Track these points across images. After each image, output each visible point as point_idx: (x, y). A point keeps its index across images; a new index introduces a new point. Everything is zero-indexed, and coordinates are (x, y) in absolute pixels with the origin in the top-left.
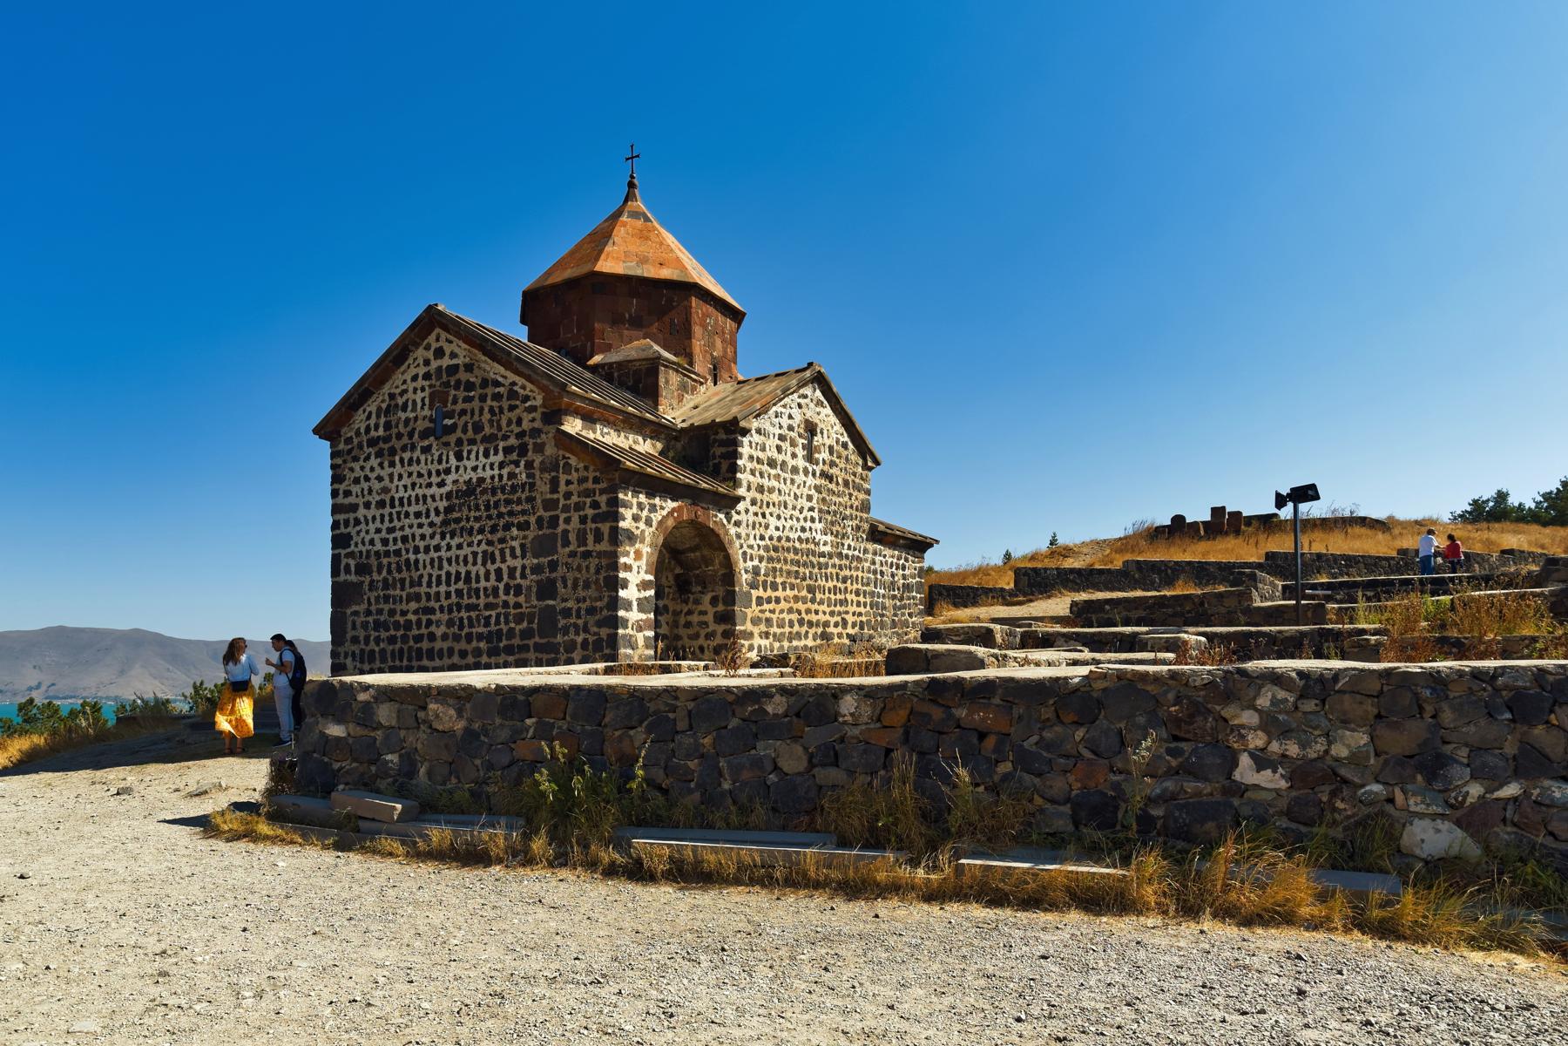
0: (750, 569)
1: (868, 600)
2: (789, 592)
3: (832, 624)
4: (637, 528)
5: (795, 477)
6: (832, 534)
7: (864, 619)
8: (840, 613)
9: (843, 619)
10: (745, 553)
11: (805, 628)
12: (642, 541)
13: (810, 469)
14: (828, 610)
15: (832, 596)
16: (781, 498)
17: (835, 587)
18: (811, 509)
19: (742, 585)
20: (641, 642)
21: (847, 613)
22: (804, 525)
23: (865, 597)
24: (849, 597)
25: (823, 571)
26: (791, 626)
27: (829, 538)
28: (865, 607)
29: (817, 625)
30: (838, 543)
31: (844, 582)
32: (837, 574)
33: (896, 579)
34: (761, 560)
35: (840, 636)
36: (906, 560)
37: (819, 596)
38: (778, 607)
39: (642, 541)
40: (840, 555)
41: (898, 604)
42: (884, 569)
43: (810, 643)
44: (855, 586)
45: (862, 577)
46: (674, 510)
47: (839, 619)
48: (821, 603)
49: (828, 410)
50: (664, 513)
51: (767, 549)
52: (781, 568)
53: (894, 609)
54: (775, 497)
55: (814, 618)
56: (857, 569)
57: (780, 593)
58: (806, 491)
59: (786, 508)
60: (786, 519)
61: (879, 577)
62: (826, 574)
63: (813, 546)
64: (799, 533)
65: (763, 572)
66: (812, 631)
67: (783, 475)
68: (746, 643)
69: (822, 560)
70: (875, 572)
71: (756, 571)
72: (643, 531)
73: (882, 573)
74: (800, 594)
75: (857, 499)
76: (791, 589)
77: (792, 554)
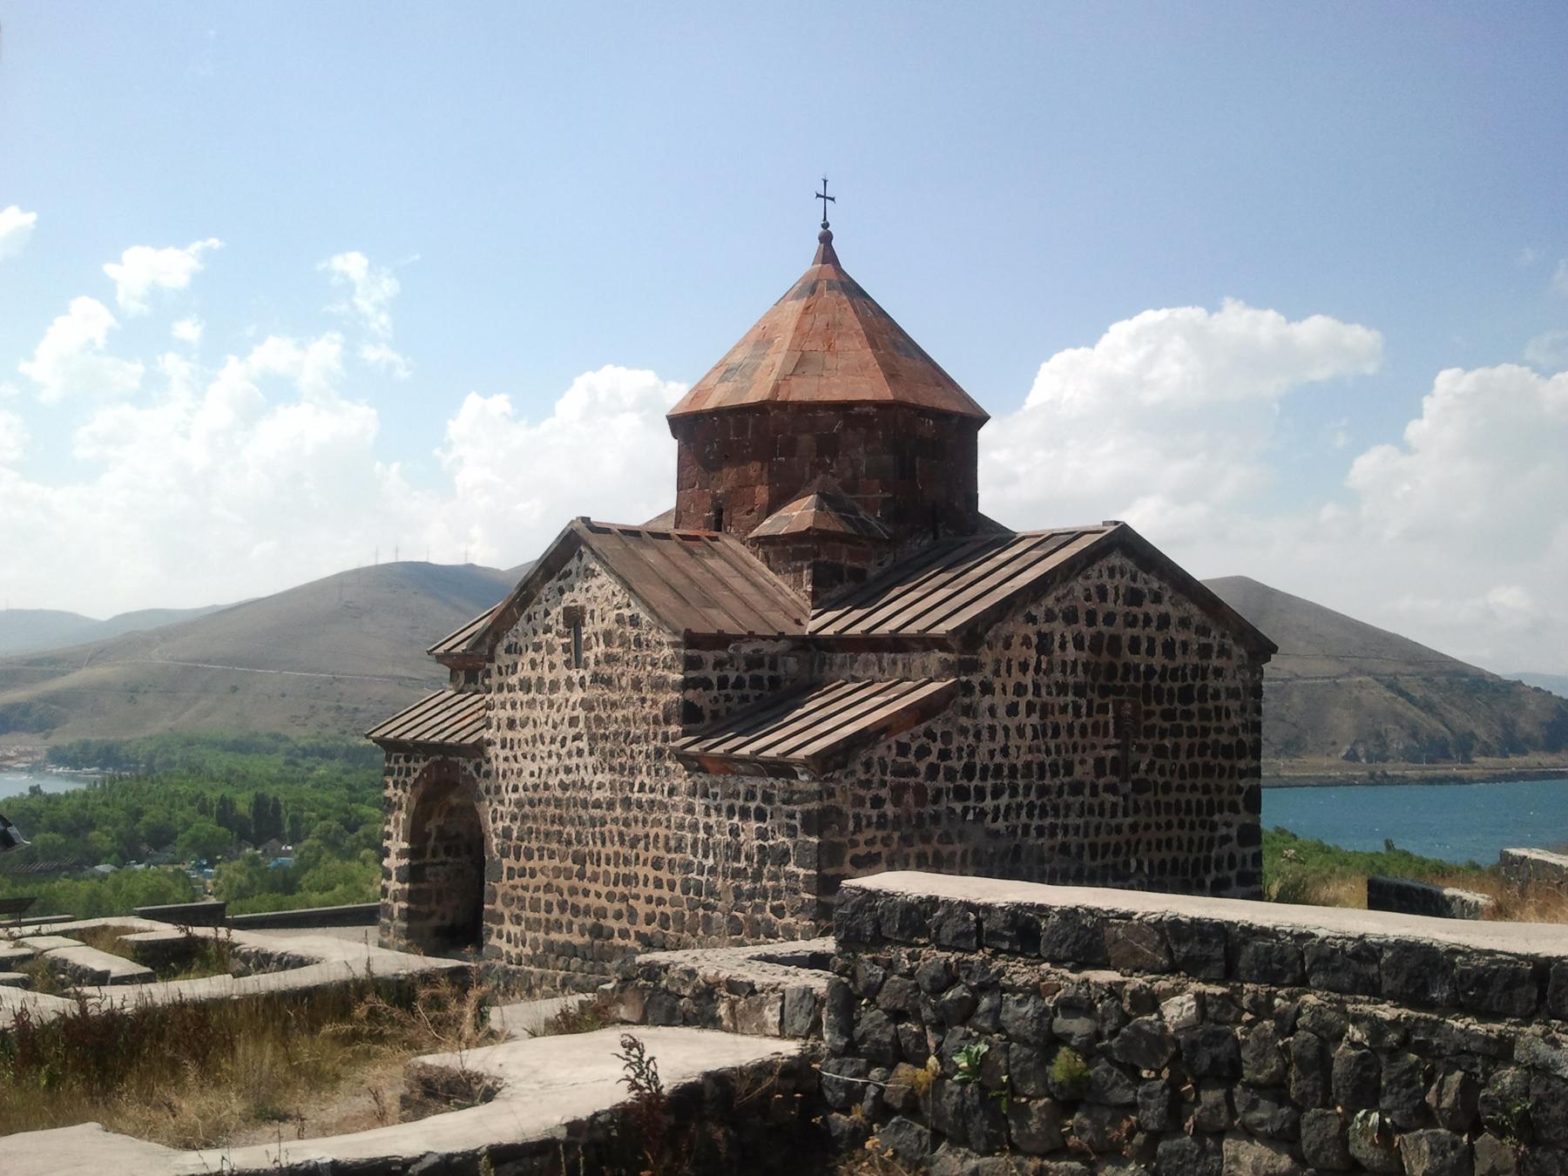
0: (500, 831)
1: (678, 877)
2: (546, 861)
3: (610, 914)
4: (396, 795)
5: (554, 697)
6: (612, 769)
7: (668, 910)
8: (624, 898)
9: (630, 908)
10: (495, 811)
11: (568, 915)
12: (400, 808)
13: (576, 679)
14: (604, 890)
15: (612, 869)
16: (539, 730)
17: (617, 854)
18: (576, 738)
19: (491, 852)
20: (396, 914)
21: (637, 897)
22: (567, 762)
23: (671, 870)
24: (642, 871)
25: (597, 829)
26: (549, 910)
27: (605, 777)
28: (672, 889)
29: (587, 912)
30: (621, 784)
31: (634, 843)
32: (621, 834)
33: (742, 837)
34: (514, 818)
35: (624, 934)
36: (768, 798)
37: (589, 869)
38: (533, 882)
39: (400, 808)
40: (627, 803)
41: (747, 886)
42: (712, 820)
43: (577, 940)
44: (653, 852)
45: (667, 838)
46: (424, 770)
47: (623, 906)
48: (595, 878)
49: (604, 578)
50: (417, 775)
51: (519, 804)
52: (538, 829)
53: (737, 897)
54: (528, 732)
55: (582, 901)
56: (657, 823)
57: (535, 863)
58: (567, 713)
59: (543, 743)
60: (542, 758)
61: (702, 835)
62: (602, 834)
63: (582, 794)
64: (562, 776)
65: (515, 834)
66: (578, 921)
67: (540, 697)
68: (495, 928)
69: (597, 813)
70: (694, 827)
71: (507, 833)
72: (400, 797)
73: (708, 828)
74: (562, 865)
75: (655, 703)
76: (550, 858)
77: (552, 808)
